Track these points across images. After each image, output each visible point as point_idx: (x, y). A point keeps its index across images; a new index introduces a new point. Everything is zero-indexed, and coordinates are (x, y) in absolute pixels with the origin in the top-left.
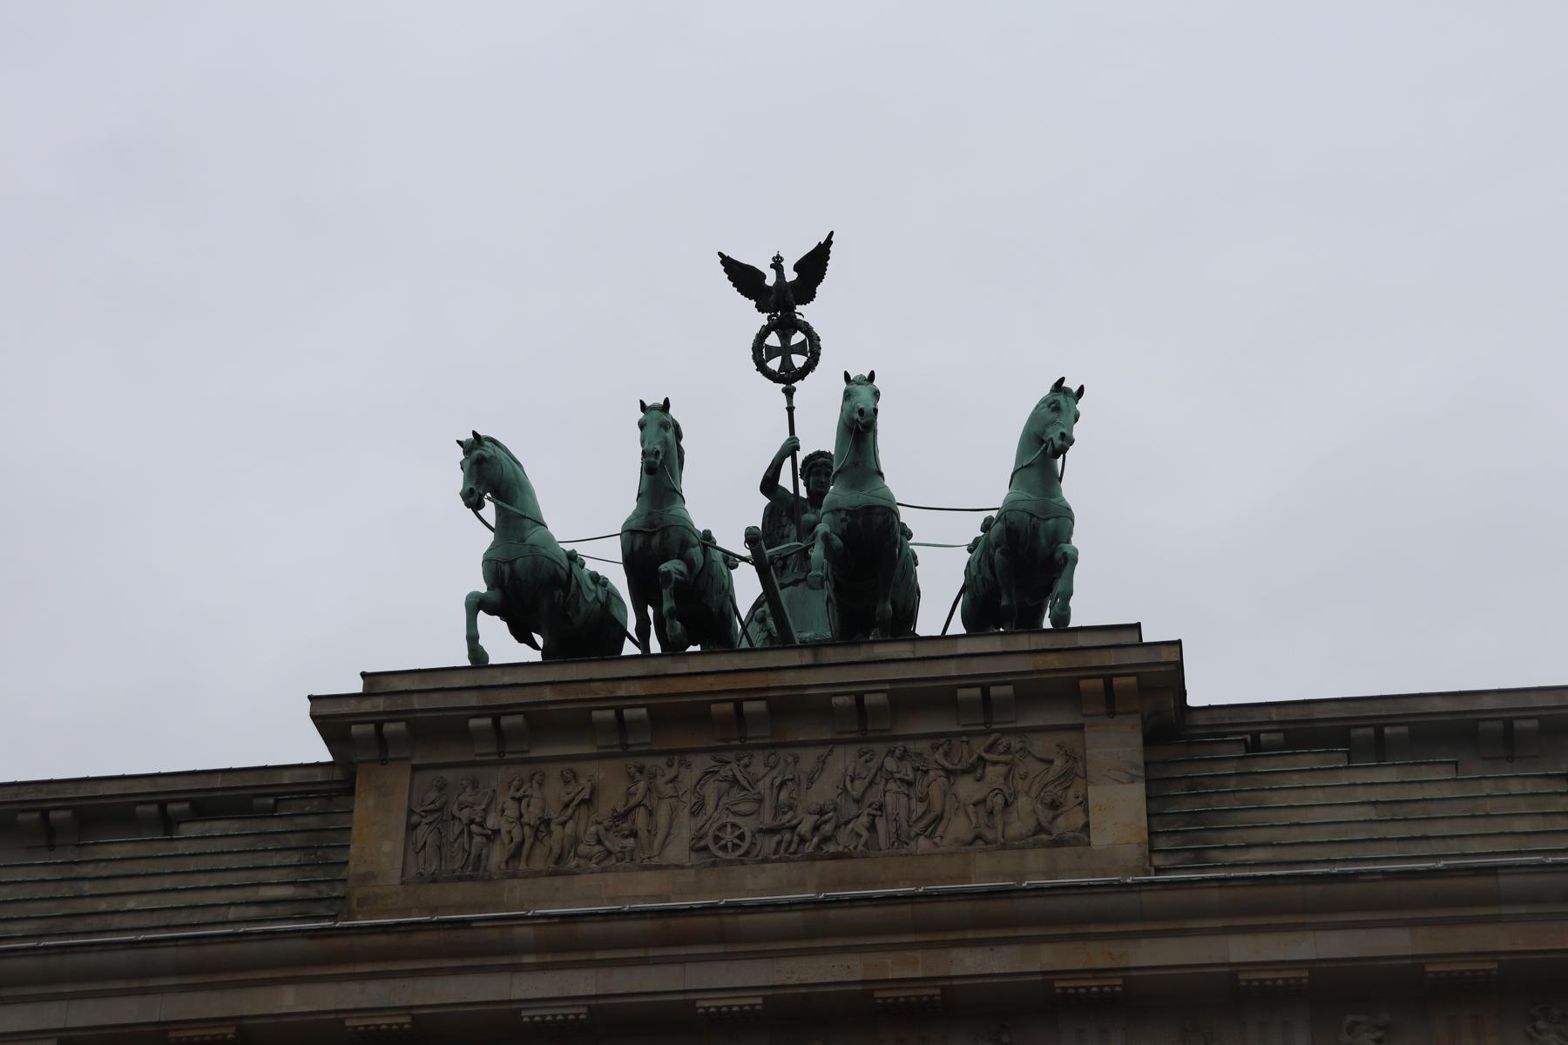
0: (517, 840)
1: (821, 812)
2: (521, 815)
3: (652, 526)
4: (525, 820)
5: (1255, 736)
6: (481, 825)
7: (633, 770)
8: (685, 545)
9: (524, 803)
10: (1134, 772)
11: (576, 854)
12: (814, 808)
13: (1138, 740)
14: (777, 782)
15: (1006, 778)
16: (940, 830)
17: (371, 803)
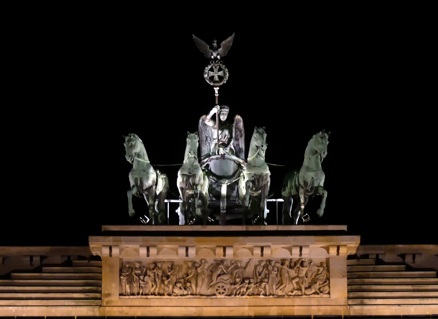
0: (154, 287)
1: (249, 283)
2: (155, 277)
3: (190, 173)
4: (157, 280)
5: (377, 255)
6: (143, 281)
7: (190, 265)
8: (200, 180)
9: (156, 273)
10: (344, 274)
11: (173, 292)
12: (247, 281)
13: (345, 262)
14: (235, 272)
15: (306, 274)
16: (286, 289)
17: (108, 269)
